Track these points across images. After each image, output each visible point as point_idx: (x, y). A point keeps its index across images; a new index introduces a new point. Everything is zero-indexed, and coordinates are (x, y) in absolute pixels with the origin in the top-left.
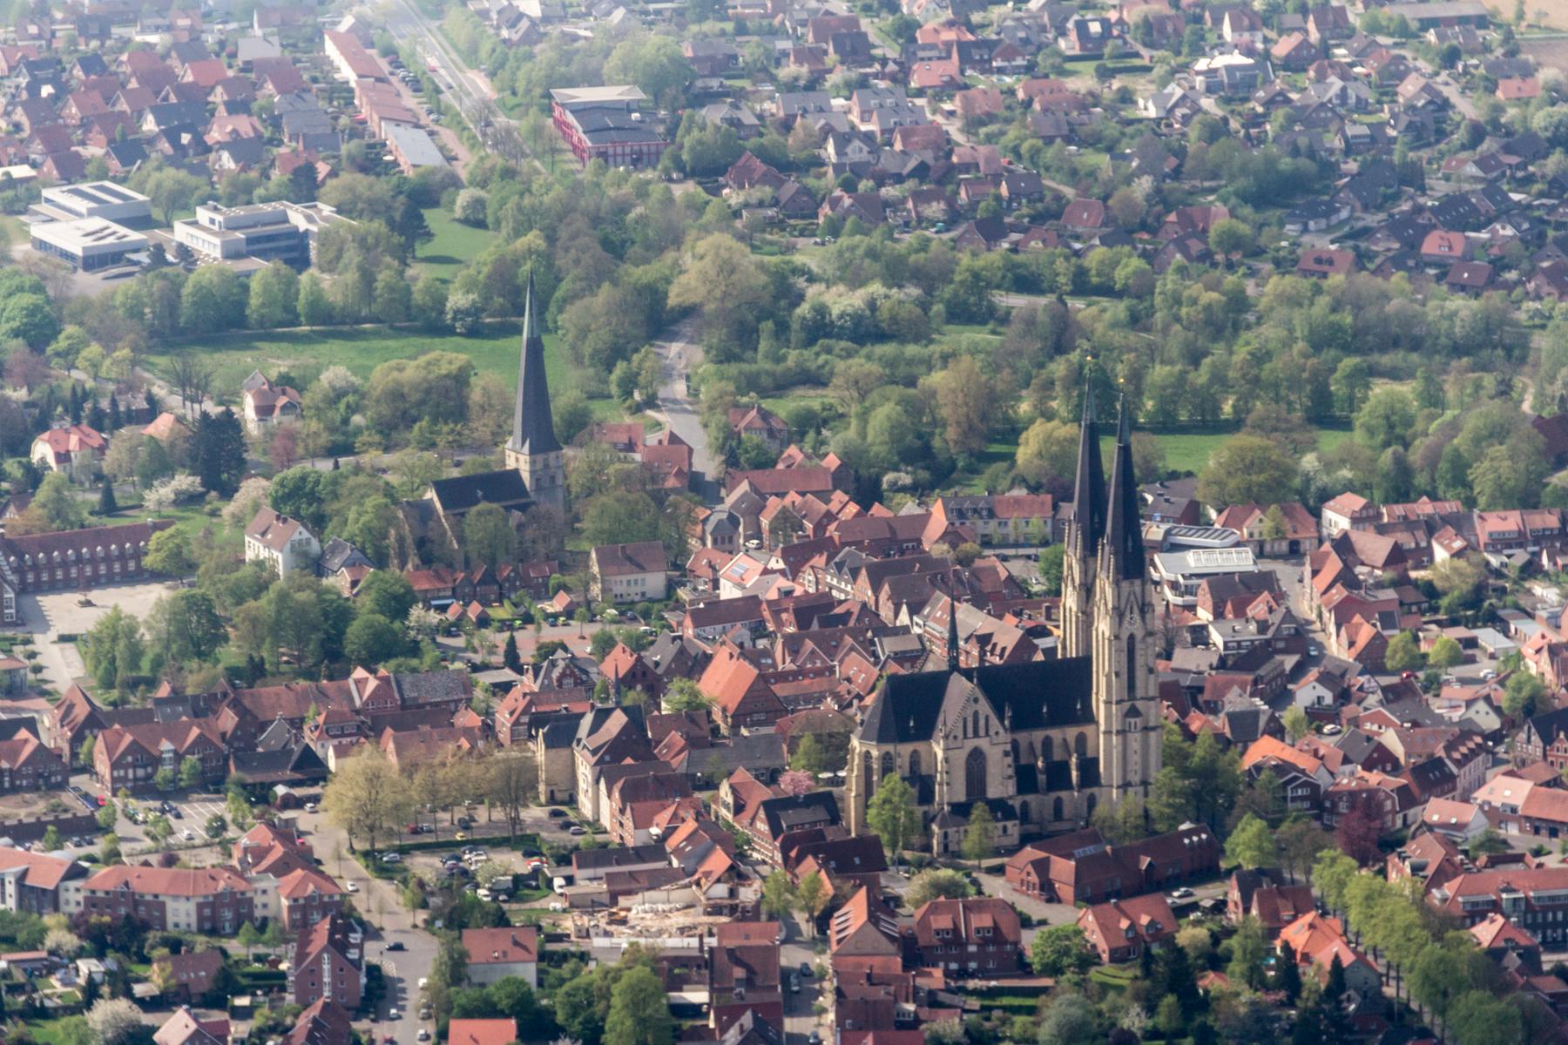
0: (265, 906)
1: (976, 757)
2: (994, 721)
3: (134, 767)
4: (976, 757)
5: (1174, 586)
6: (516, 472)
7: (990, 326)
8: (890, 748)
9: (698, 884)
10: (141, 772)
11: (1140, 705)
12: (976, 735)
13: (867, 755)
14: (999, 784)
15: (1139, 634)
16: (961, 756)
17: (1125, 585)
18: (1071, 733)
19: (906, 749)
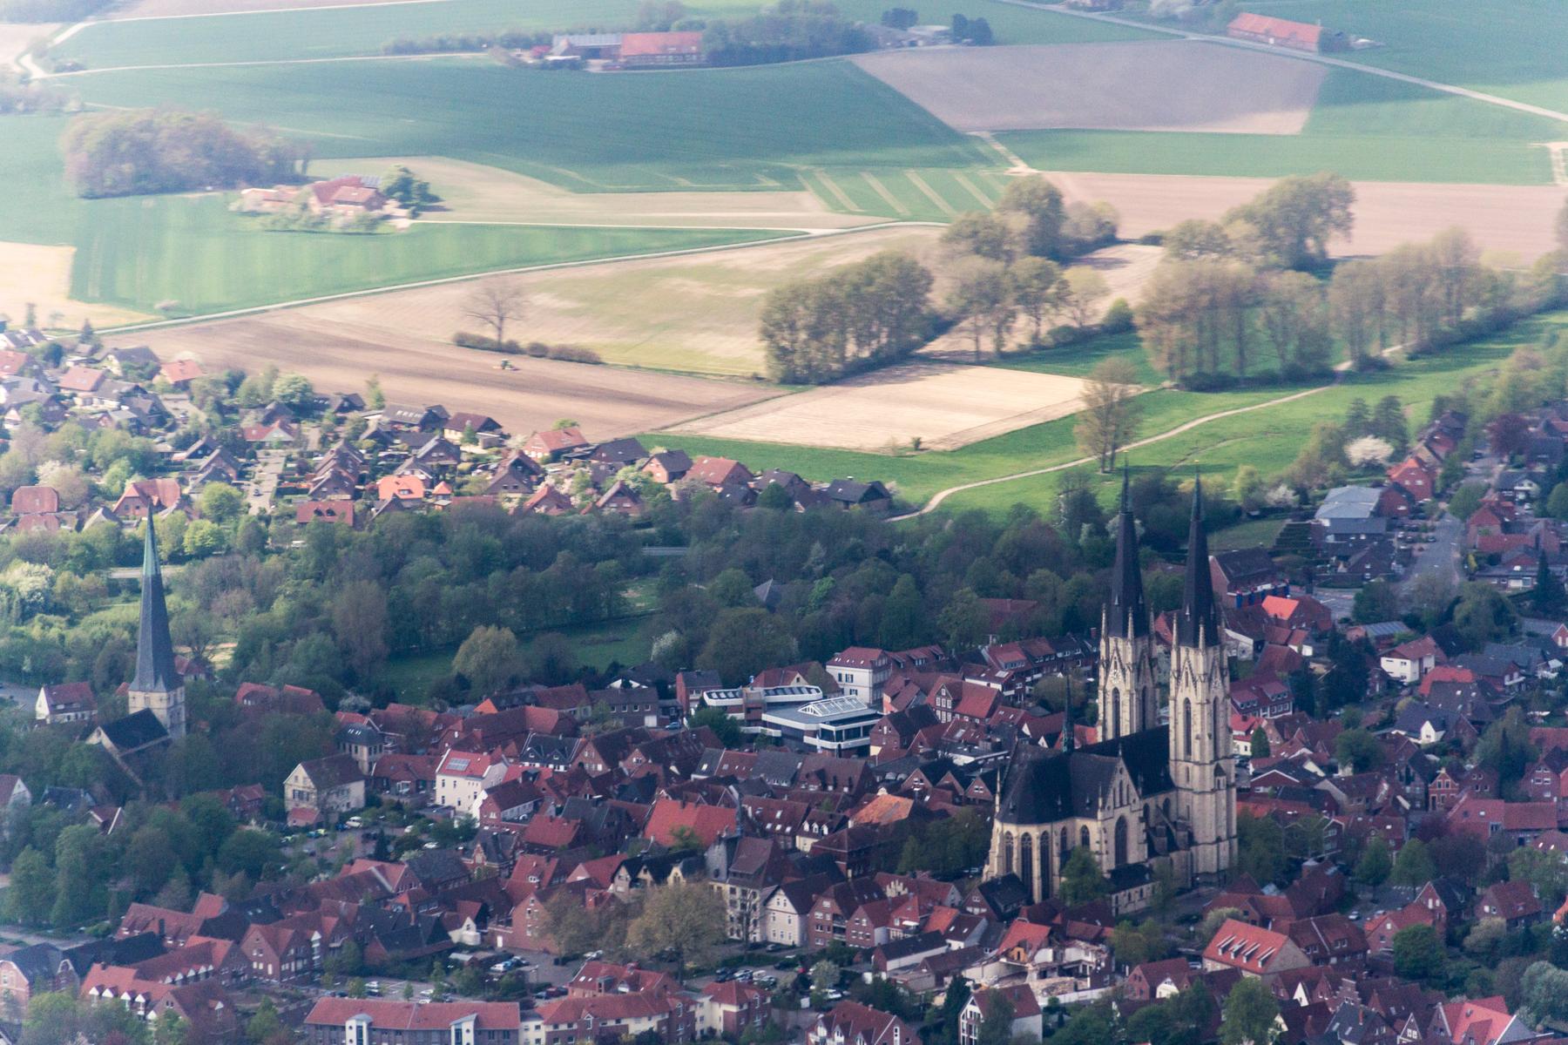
0: (702, 1019)
1: (1122, 824)
2: (1133, 790)
3: (297, 959)
4: (1122, 824)
5: (825, 735)
6: (147, 714)
7: (124, 594)
8: (1047, 827)
9: (1006, 954)
10: (300, 965)
11: (1222, 763)
12: (1122, 805)
13: (1026, 838)
14: (1136, 853)
15: (1221, 696)
16: (1112, 824)
17: (1211, 651)
18: (1161, 798)
19: (1058, 826)
